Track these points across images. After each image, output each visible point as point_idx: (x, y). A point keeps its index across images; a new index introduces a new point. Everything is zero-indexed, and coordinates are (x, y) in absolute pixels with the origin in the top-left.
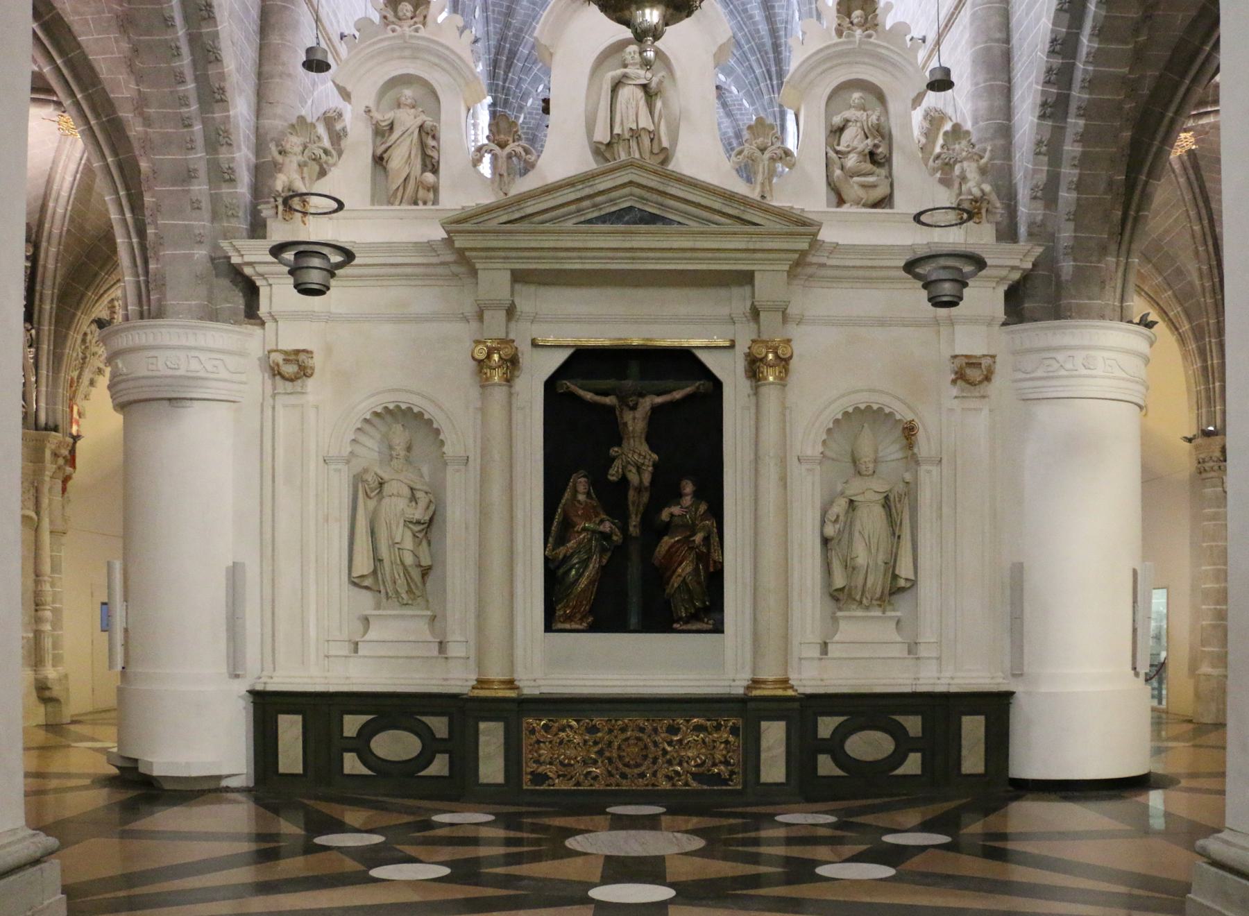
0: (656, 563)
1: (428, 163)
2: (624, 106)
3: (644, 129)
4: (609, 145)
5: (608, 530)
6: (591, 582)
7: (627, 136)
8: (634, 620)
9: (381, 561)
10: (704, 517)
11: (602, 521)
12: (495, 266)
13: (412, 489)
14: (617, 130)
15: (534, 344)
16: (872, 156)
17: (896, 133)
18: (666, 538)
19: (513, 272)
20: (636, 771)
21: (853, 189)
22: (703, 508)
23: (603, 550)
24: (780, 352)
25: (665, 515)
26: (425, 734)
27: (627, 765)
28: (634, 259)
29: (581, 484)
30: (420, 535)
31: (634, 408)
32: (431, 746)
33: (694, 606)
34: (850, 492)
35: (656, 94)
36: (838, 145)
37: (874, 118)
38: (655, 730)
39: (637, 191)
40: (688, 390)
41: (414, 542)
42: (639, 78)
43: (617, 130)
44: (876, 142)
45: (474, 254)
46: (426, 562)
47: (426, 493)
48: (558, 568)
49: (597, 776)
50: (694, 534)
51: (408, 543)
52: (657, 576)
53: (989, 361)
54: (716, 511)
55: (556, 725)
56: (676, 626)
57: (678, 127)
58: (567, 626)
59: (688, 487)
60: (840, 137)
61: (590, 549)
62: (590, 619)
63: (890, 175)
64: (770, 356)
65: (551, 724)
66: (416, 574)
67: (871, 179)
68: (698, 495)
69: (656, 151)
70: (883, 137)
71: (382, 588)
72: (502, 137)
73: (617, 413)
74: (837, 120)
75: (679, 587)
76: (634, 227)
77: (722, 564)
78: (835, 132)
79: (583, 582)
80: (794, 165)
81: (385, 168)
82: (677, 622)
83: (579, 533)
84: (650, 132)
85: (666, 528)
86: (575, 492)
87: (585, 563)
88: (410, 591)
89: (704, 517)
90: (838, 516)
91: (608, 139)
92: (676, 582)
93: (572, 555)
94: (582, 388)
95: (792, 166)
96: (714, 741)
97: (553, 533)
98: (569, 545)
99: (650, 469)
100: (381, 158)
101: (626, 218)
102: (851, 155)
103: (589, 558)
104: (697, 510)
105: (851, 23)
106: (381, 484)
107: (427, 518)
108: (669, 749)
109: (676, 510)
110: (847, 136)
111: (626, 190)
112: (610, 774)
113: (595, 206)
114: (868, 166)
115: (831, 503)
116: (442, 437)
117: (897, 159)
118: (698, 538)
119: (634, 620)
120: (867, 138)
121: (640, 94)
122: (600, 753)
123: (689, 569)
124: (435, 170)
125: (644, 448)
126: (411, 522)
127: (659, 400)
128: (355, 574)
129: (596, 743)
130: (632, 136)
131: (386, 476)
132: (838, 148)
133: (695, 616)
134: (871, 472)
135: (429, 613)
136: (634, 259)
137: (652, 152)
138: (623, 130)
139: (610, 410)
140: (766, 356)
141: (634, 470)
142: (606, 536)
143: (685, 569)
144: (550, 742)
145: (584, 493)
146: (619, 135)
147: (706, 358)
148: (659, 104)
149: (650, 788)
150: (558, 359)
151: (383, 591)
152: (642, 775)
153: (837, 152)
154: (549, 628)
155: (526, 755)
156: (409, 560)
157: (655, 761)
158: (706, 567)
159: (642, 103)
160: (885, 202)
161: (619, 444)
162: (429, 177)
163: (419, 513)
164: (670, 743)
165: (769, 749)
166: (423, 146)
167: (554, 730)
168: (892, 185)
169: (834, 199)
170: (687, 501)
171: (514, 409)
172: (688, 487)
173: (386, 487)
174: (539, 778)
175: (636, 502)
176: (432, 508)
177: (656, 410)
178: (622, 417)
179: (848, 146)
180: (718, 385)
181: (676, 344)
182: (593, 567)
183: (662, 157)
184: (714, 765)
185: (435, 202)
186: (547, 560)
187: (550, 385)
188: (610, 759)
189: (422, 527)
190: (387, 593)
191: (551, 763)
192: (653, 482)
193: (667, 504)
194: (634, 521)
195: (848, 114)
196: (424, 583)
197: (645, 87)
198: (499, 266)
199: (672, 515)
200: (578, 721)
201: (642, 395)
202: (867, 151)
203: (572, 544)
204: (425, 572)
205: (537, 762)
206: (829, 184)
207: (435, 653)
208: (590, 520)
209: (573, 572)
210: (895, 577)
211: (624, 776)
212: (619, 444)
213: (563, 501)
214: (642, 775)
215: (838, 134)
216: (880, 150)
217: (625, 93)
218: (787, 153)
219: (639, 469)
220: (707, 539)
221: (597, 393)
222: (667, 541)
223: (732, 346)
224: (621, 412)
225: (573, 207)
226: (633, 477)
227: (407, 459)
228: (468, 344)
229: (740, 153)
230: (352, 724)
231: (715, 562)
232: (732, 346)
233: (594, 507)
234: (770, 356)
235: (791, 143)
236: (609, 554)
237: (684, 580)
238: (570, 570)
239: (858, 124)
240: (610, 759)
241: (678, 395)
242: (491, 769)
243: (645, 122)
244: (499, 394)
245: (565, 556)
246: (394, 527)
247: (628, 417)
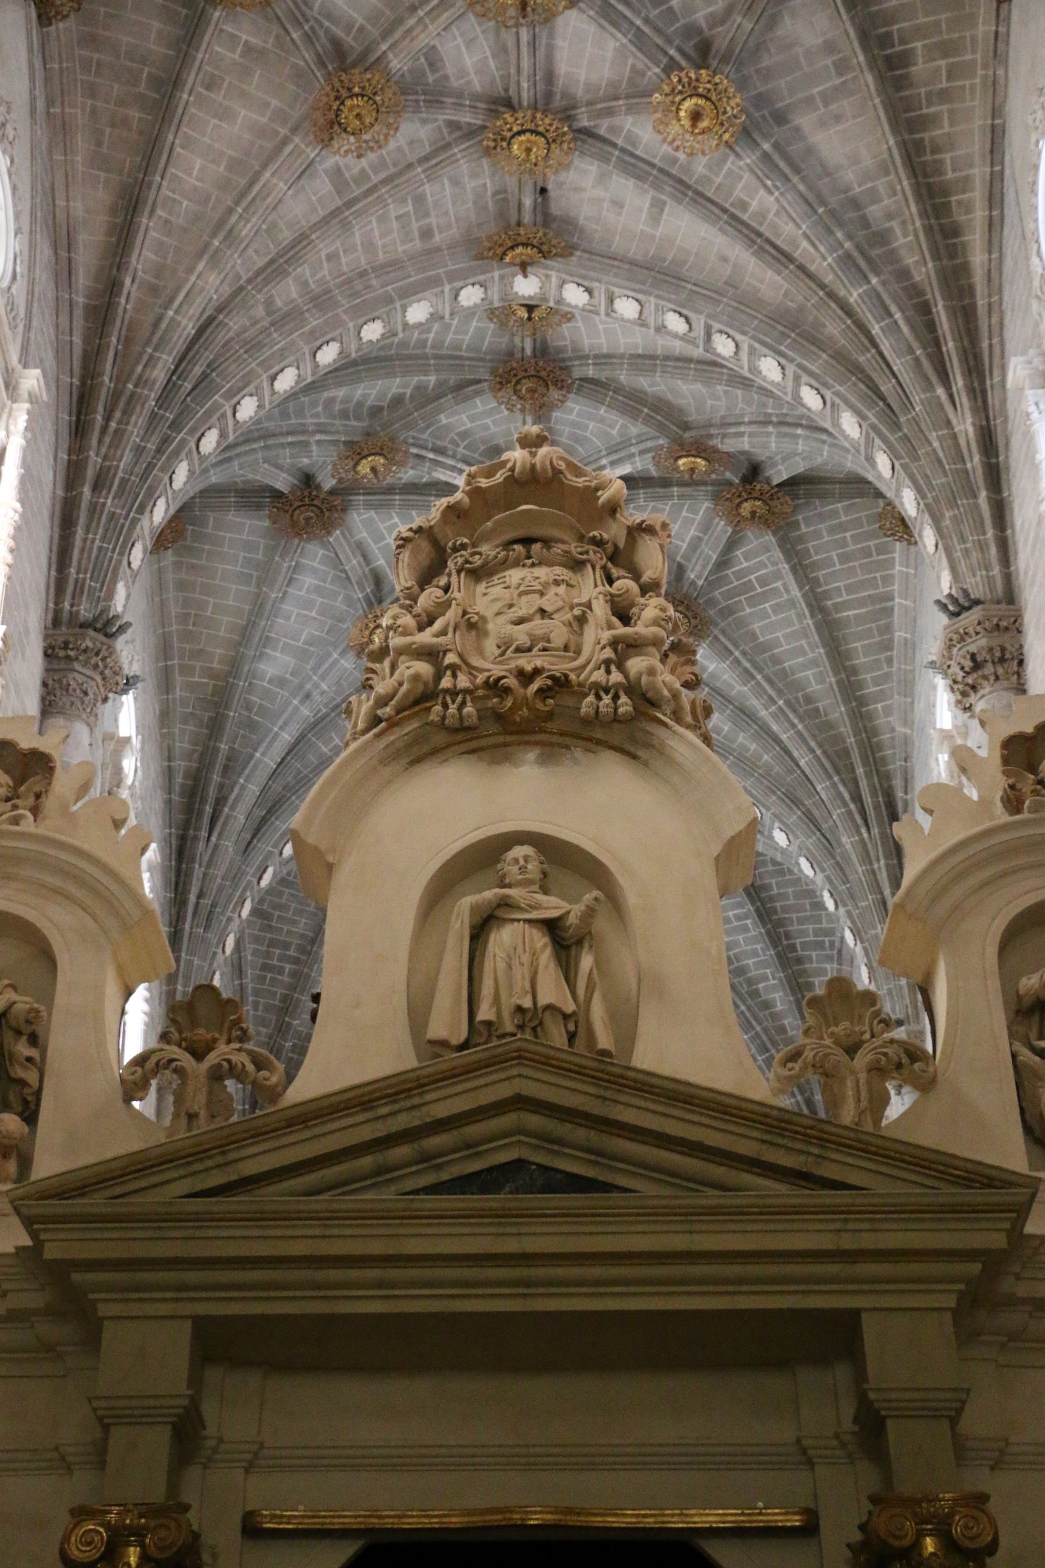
2: (501, 965)
3: (549, 1007)
7: (509, 1028)
12: (151, 1309)
14: (484, 1013)
19: (203, 1328)
24: (957, 1531)
28: (527, 1283)
35: (580, 942)
39: (534, 1121)
42: (533, 907)
43: (484, 1013)
45: (91, 1277)
57: (635, 1018)
64: (930, 1545)
84: (566, 1017)
91: (464, 1035)
111: (508, 1120)
113: (425, 1158)
121: (540, 940)
130: (521, 1027)
136: (527, 1283)
138: (499, 1014)
140: (917, 1544)
146: (488, 1024)
159: (546, 956)
181: (650, 1522)
197: (552, 926)
198: (164, 1309)
223: (810, 1529)
232: (810, 1529)
234: (930, 1545)
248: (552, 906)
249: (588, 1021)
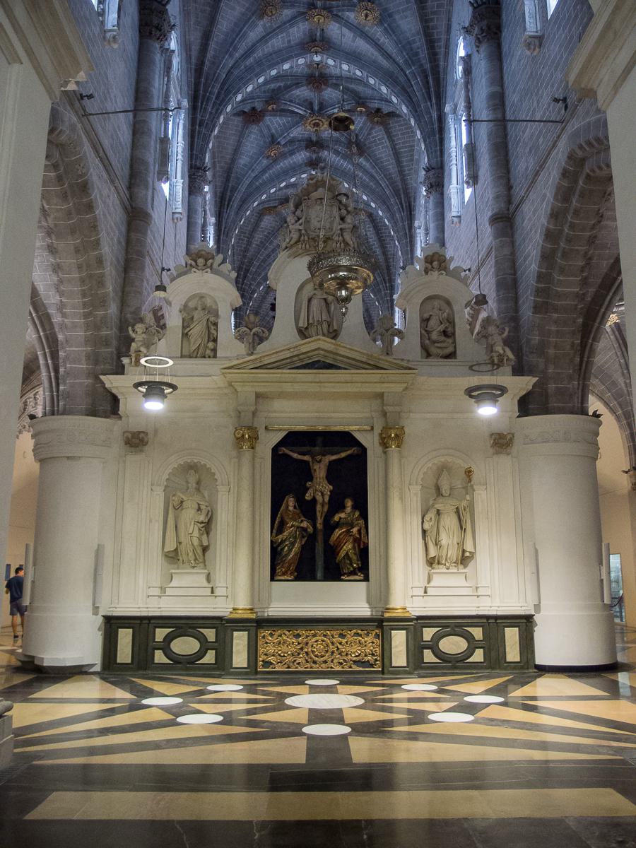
0: (331, 543)
4: (307, 328)
6: (296, 554)
8: (319, 575)
9: (180, 543)
10: (357, 519)
11: (302, 521)
13: (199, 504)
14: (311, 321)
16: (445, 333)
18: (337, 530)
20: (322, 659)
22: (357, 514)
25: (336, 518)
26: (202, 639)
29: (291, 502)
31: (320, 461)
32: (205, 646)
34: (437, 506)
38: (332, 636)
40: (349, 452)
46: (205, 543)
47: (207, 506)
48: (279, 546)
50: (352, 527)
51: (196, 534)
52: (331, 551)
53: (511, 436)
54: (364, 516)
58: (283, 578)
59: (349, 503)
62: (296, 574)
63: (454, 342)
66: (199, 551)
67: (443, 345)
68: (354, 507)
69: (331, 331)
70: (450, 323)
71: (180, 558)
73: (311, 464)
76: (321, 371)
77: (368, 544)
82: (343, 575)
85: (337, 525)
86: (287, 506)
87: (293, 544)
88: (196, 559)
89: (357, 519)
92: (342, 554)
94: (291, 451)
97: (275, 528)
98: (285, 534)
99: (329, 493)
100: (187, 334)
101: (316, 366)
103: (295, 541)
106: (182, 502)
107: (207, 520)
109: (343, 515)
110: (432, 323)
112: (307, 661)
114: (443, 338)
118: (355, 530)
120: (441, 323)
122: (302, 649)
123: (350, 546)
124: (215, 341)
126: (198, 522)
127: (334, 457)
128: (166, 550)
129: (299, 644)
132: (427, 329)
135: (206, 571)
137: (329, 332)
139: (306, 463)
141: (320, 494)
142: (305, 530)
147: (358, 436)
149: (329, 669)
152: (325, 662)
153: (426, 331)
154: (272, 579)
155: (261, 650)
156: (196, 542)
158: (359, 546)
160: (452, 355)
161: (311, 480)
162: (211, 345)
163: (202, 518)
164: (340, 643)
165: (396, 647)
168: (455, 347)
169: (425, 354)
170: (349, 510)
172: (349, 503)
174: (267, 664)
175: (320, 510)
177: (330, 462)
178: (313, 466)
182: (297, 545)
183: (334, 334)
184: (366, 656)
186: (272, 541)
187: (275, 450)
188: (307, 653)
191: (273, 655)
192: (329, 500)
193: (337, 512)
194: (320, 521)
196: (204, 555)
199: (340, 518)
201: (324, 455)
203: (286, 533)
204: (205, 549)
206: (422, 346)
208: (295, 521)
210: (464, 551)
211: (315, 662)
212: (311, 480)
214: (325, 662)
219: (323, 494)
220: (359, 531)
222: (338, 532)
224: (313, 463)
225: (289, 360)
226: (319, 498)
227: (198, 490)
231: (364, 543)
236: (306, 538)
237: (347, 554)
241: (343, 455)
242: (240, 658)
244: (247, 454)
245: (282, 540)
246: (188, 525)
247: (316, 467)
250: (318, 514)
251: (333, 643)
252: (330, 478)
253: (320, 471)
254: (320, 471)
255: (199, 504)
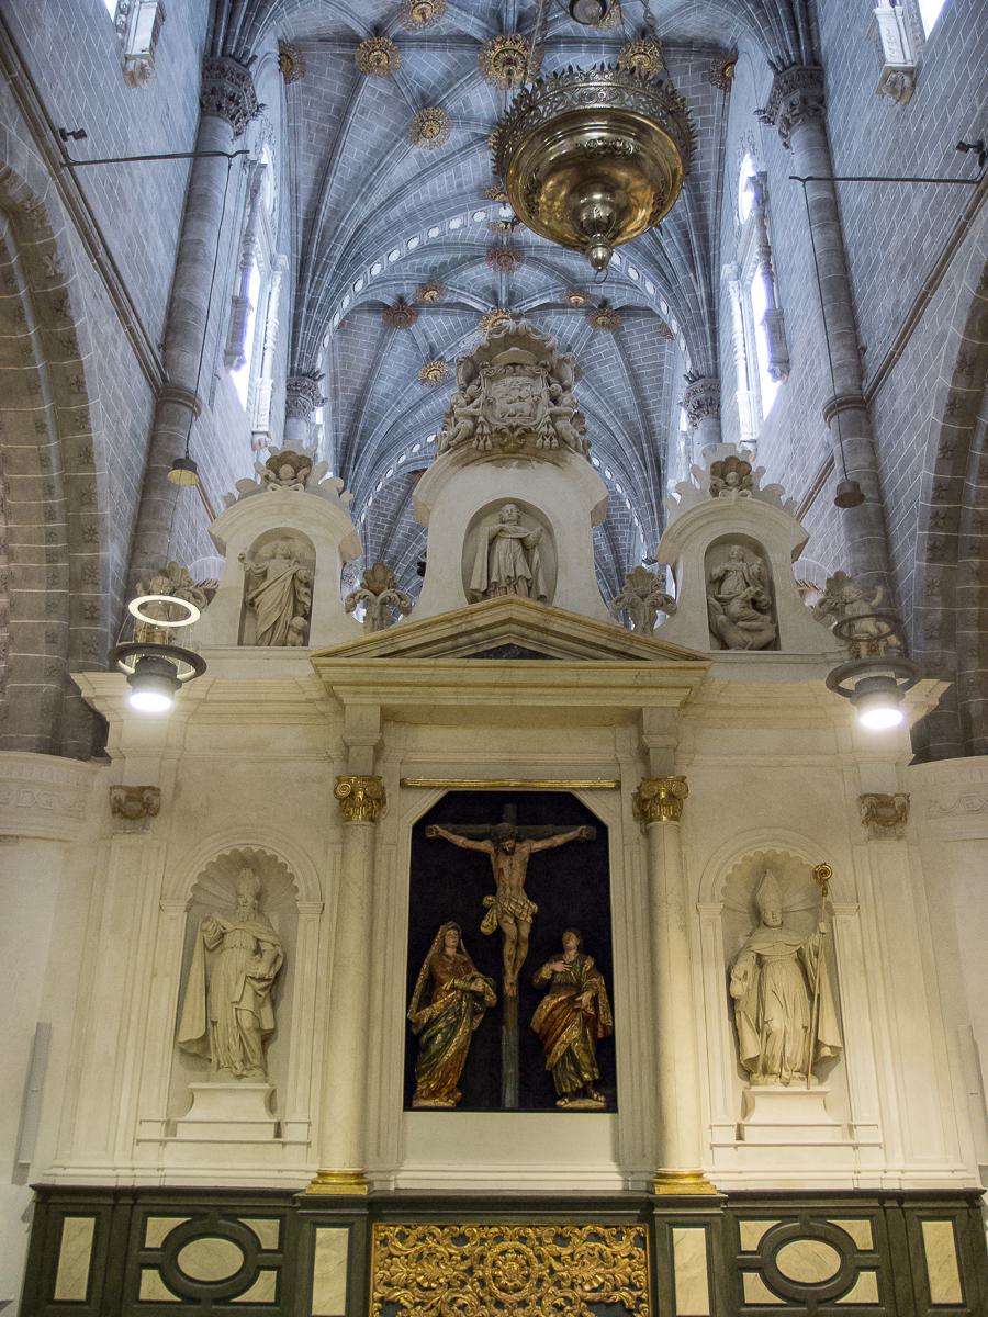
0: (535, 1027)
1: (300, 609)
2: (501, 557)
5: (480, 989)
6: (459, 1051)
7: (504, 584)
8: (510, 1095)
9: (214, 1023)
10: (590, 975)
11: (473, 979)
14: (494, 578)
15: (403, 784)
16: (754, 603)
17: (777, 581)
18: (547, 998)
20: (516, 1297)
21: (735, 635)
22: (589, 963)
23: (475, 1013)
25: (546, 973)
27: (503, 1289)
29: (450, 937)
30: (263, 994)
33: (581, 1078)
34: (758, 947)
35: (533, 547)
36: (719, 593)
37: (755, 568)
38: (539, 1239)
40: (571, 835)
41: (255, 999)
43: (494, 578)
44: (758, 589)
47: (274, 945)
49: (465, 1305)
50: (580, 993)
51: (248, 1003)
52: (535, 1045)
54: (605, 968)
55: (414, 1233)
56: (558, 1103)
59: (572, 941)
60: (720, 586)
61: (460, 1010)
63: (774, 620)
65: (407, 1231)
66: (254, 1040)
67: (754, 624)
68: (584, 950)
71: (213, 1057)
72: (375, 586)
73: (492, 859)
74: (717, 571)
75: (563, 1057)
77: (613, 1027)
78: (715, 582)
79: (452, 1049)
80: (675, 611)
81: (255, 612)
82: (559, 1098)
83: (449, 992)
84: (527, 581)
85: (548, 987)
86: (443, 947)
87: (453, 1028)
88: (245, 1060)
89: (590, 975)
90: (746, 974)
92: (559, 1049)
93: (437, 1020)
94: (454, 832)
95: (672, 613)
96: (614, 1255)
99: (529, 919)
100: (252, 603)
102: (734, 601)
103: (459, 1022)
104: (582, 966)
105: (726, 483)
106: (223, 935)
107: (272, 974)
108: (556, 1266)
109: (559, 967)
110: (729, 585)
114: (752, 612)
115: (736, 958)
116: (295, 883)
117: (780, 605)
118: (585, 998)
119: (510, 1095)
120: (748, 585)
121: (517, 546)
123: (575, 1034)
124: (307, 616)
125: (522, 898)
127: (539, 845)
128: (182, 1038)
129: (464, 1258)
131: (229, 927)
133: (582, 1093)
134: (779, 923)
135: (266, 1086)
139: (485, 856)
141: (511, 921)
142: (478, 997)
143: (571, 1035)
144: (407, 1256)
145: (452, 947)
147: (589, 801)
148: (536, 556)
150: (427, 802)
151: (214, 1060)
153: (718, 600)
154: (408, 1105)
155: (378, 1274)
156: (247, 1021)
157: (540, 1280)
158: (594, 1034)
159: (520, 554)
160: (773, 644)
162: (299, 621)
163: (262, 969)
164: (558, 1258)
166: (295, 592)
167: (411, 1240)
170: (571, 955)
171: (378, 851)
172: (572, 941)
173: (227, 938)
175: (513, 956)
176: (280, 962)
177: (534, 857)
179: (730, 593)
180: (602, 829)
182: (462, 1034)
184: (616, 1289)
185: (305, 643)
186: (408, 1023)
187: (419, 829)
188: (482, 1281)
189: (267, 983)
190: (219, 1062)
191: (406, 1287)
193: (547, 959)
194: (511, 978)
195: (727, 566)
197: (522, 541)
199: (554, 973)
200: (442, 1228)
201: (519, 840)
202: (750, 597)
203: (438, 1005)
204: (267, 1038)
205: (388, 1284)
206: (711, 631)
207: (271, 1137)
208: (459, 976)
209: (439, 1036)
213: (430, 955)
215: (717, 584)
216: (763, 597)
217: (502, 545)
218: (668, 599)
220: (595, 1000)
221: (470, 837)
222: (549, 1003)
226: (510, 929)
228: (331, 782)
229: (620, 600)
230: (158, 1230)
231: (604, 1027)
233: (464, 963)
235: (671, 590)
238: (436, 1034)
239: (739, 574)
240: (482, 1281)
241: (559, 840)
243: (522, 570)
245: (430, 1018)
247: (504, 863)
248: (522, 532)
249: (536, 583)
250: (508, 964)
251: (540, 1258)
252: (531, 888)
253: (512, 872)
254: (512, 872)
255: (258, 940)
